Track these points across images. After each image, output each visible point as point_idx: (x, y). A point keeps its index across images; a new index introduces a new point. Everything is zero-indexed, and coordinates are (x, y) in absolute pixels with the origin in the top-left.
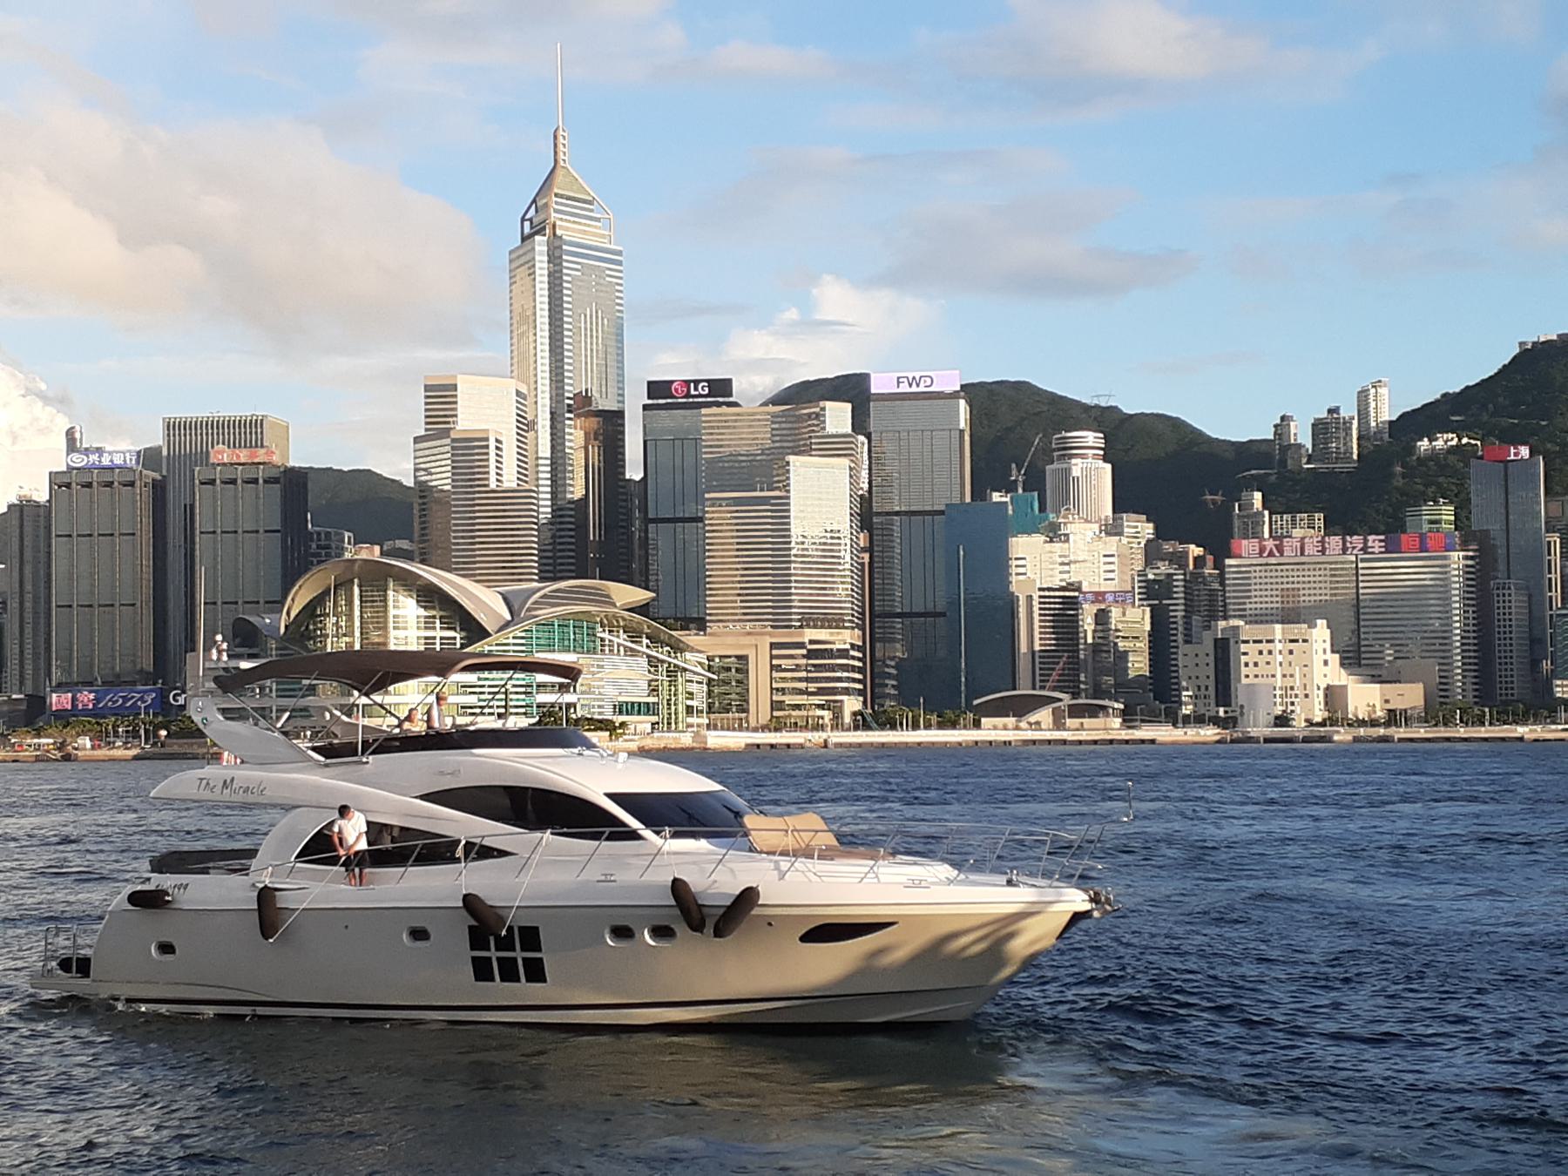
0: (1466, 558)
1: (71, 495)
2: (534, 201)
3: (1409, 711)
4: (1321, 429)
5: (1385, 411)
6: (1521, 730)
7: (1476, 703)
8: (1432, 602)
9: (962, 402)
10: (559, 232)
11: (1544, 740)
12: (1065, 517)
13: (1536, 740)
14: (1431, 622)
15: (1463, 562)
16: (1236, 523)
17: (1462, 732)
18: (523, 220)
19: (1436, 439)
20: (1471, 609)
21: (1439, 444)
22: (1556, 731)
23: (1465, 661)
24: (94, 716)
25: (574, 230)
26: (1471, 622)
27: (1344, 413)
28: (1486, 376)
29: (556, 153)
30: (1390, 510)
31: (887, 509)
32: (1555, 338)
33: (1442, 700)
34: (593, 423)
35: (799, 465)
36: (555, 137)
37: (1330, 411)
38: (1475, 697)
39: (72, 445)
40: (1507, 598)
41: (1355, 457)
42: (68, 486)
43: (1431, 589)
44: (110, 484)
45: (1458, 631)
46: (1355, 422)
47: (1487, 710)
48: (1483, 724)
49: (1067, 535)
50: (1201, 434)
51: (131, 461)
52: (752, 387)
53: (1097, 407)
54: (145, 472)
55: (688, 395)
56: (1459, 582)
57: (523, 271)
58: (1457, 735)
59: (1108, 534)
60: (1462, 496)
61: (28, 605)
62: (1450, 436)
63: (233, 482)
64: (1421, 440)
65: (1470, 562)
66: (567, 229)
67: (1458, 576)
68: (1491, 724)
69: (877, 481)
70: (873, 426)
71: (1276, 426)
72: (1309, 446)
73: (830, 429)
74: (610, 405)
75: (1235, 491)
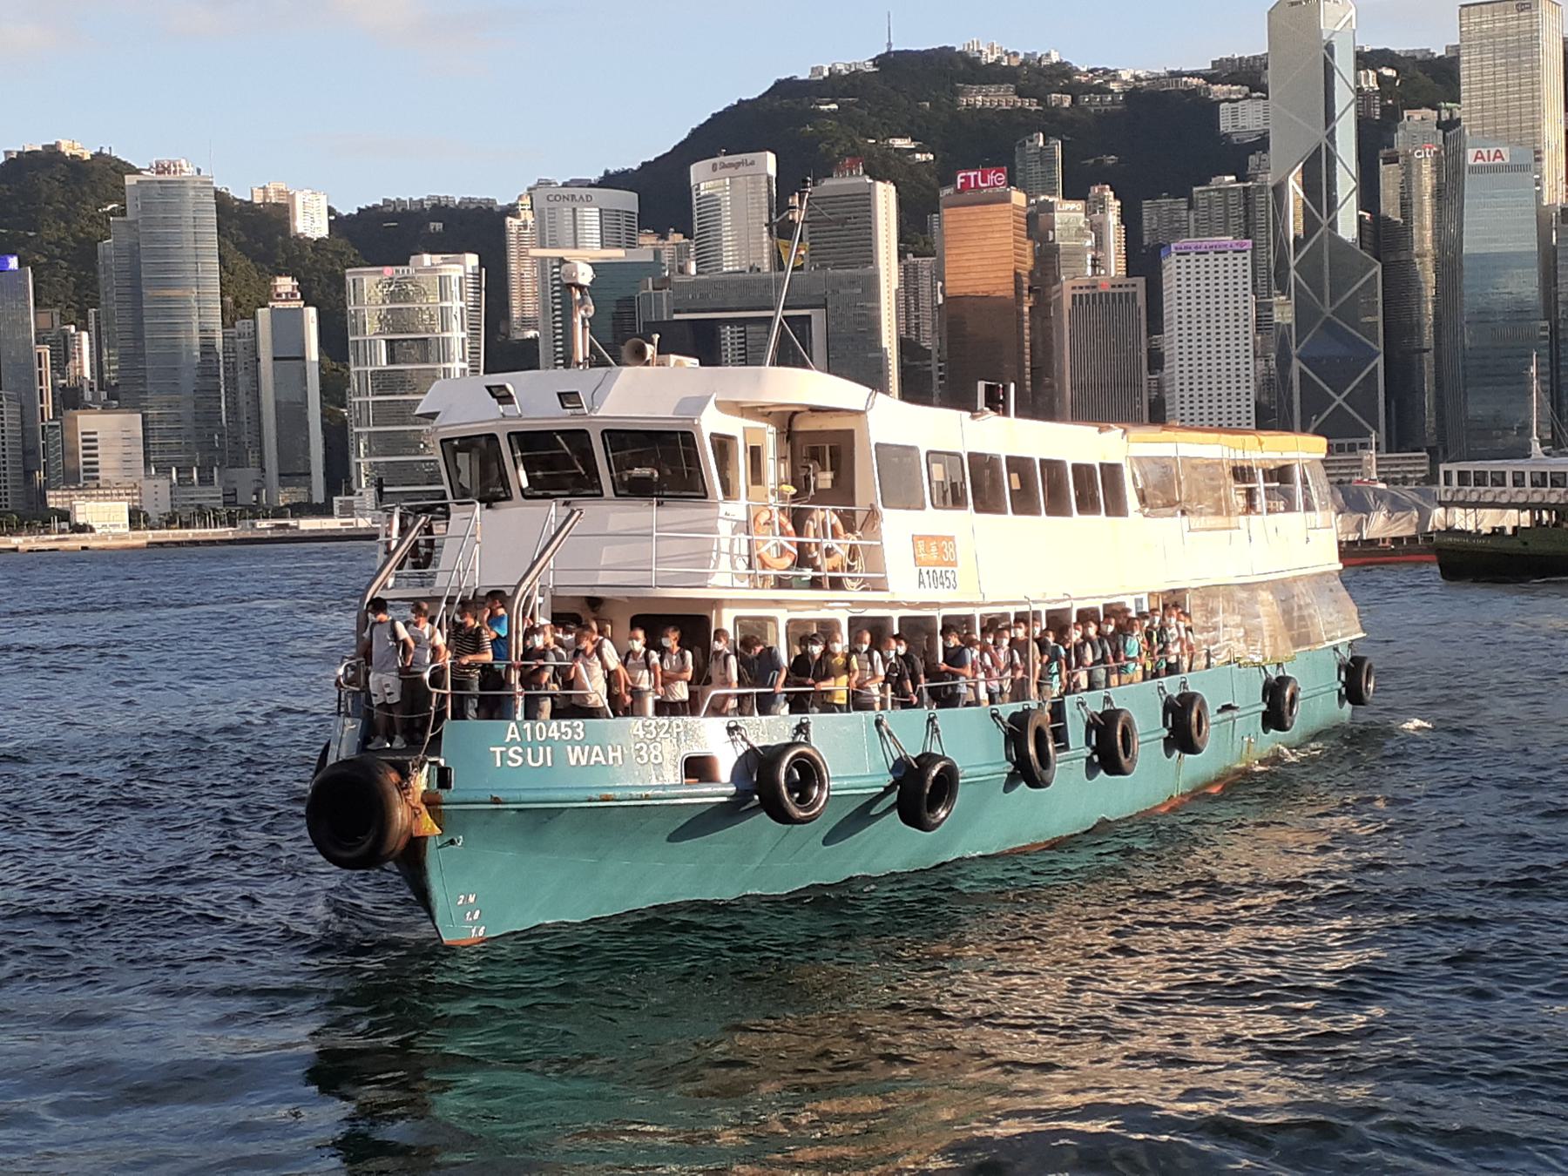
6: (16, 541)
13: (30, 551)
22: (50, 541)
32: (40, 149)
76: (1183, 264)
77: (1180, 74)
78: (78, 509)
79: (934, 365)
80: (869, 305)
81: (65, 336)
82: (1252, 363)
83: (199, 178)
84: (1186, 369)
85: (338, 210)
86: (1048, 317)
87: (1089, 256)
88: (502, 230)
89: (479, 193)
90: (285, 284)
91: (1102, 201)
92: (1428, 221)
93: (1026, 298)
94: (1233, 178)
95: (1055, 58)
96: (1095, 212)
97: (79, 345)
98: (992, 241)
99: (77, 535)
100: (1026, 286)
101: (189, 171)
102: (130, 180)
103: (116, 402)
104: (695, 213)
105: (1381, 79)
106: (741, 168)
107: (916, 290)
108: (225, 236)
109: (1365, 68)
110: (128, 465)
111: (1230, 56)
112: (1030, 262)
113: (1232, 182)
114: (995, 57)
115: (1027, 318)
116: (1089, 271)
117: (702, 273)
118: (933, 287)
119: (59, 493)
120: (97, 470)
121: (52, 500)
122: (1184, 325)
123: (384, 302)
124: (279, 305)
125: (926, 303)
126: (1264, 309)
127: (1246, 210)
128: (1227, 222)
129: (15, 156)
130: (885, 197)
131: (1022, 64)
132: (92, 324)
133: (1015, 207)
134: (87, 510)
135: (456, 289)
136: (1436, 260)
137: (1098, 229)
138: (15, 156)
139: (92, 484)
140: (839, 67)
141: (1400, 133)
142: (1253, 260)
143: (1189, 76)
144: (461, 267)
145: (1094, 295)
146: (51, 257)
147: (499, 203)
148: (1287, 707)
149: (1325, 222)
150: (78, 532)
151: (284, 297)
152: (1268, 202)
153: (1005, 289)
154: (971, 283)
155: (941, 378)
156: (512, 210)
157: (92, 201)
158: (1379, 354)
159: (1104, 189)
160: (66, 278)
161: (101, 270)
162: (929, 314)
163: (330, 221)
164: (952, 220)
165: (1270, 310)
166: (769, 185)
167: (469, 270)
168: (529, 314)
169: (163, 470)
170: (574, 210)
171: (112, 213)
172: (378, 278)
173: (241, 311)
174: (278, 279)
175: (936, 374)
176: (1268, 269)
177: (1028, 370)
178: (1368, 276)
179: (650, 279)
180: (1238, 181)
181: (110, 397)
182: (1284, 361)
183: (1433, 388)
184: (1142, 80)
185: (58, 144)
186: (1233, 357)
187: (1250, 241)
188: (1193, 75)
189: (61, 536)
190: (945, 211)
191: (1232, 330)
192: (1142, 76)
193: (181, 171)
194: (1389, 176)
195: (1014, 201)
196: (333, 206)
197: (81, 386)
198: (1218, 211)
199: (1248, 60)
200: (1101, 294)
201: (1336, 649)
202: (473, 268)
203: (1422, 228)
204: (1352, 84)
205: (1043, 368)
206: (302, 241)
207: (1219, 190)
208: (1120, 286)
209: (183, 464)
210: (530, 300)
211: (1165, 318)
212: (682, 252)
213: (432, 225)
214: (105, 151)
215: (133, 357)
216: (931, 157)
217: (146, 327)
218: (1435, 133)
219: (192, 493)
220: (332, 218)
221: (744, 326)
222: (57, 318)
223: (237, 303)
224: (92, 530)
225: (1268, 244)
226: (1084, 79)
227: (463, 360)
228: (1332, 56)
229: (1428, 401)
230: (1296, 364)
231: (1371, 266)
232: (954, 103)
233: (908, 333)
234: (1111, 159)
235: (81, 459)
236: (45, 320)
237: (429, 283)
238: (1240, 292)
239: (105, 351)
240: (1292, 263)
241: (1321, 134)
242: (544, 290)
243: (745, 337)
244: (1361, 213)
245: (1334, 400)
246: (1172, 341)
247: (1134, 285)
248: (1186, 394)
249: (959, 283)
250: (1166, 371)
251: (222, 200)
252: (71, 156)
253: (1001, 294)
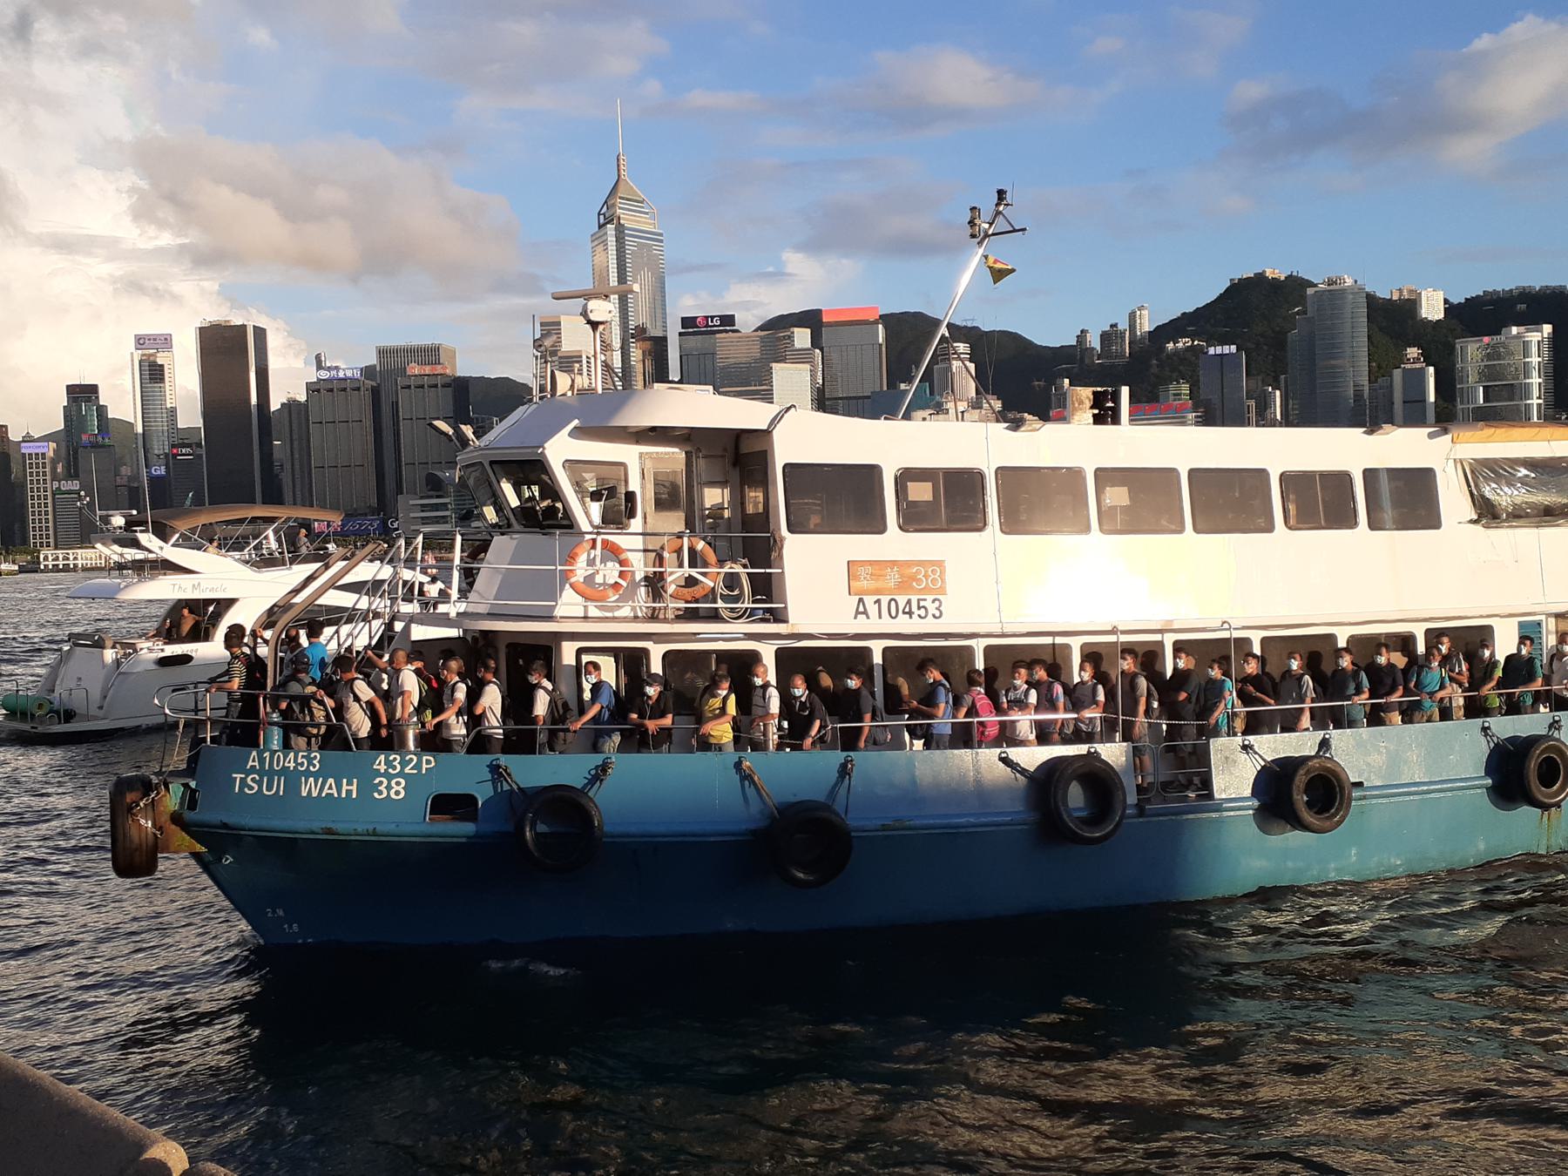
1: (320, 398)
2: (606, 202)
4: (1105, 337)
5: (1146, 325)
9: (880, 326)
10: (622, 221)
12: (946, 398)
16: (1053, 398)
18: (599, 214)
21: (1180, 345)
24: (342, 536)
25: (632, 221)
27: (1120, 327)
29: (619, 170)
30: (1150, 388)
31: (835, 395)
34: (648, 344)
35: (777, 368)
36: (618, 160)
37: (1111, 326)
39: (319, 367)
41: (1127, 355)
42: (318, 391)
44: (344, 390)
46: (1127, 333)
49: (947, 410)
50: (1031, 343)
51: (357, 374)
52: (748, 321)
53: (966, 327)
54: (366, 381)
55: (707, 326)
57: (601, 248)
59: (973, 408)
61: (297, 467)
63: (422, 387)
66: (627, 220)
69: (828, 378)
70: (824, 342)
71: (1078, 337)
72: (1099, 348)
73: (798, 345)
74: (660, 334)
75: (1053, 378)
85: (1451, 300)
90: (1413, 352)
101: (1349, 282)
102: (1310, 291)
124: (1408, 366)
135: (1534, 349)
144: (1540, 334)
163: (1445, 308)
167: (1546, 335)
171: (1298, 313)
172: (1478, 346)
173: (1382, 371)
185: (1264, 272)
206: (1426, 322)
213: (1519, 306)
222: (1260, 383)
223: (1379, 367)
227: (1539, 398)
237: (1516, 347)
239: (1291, 401)
251: (1371, 299)
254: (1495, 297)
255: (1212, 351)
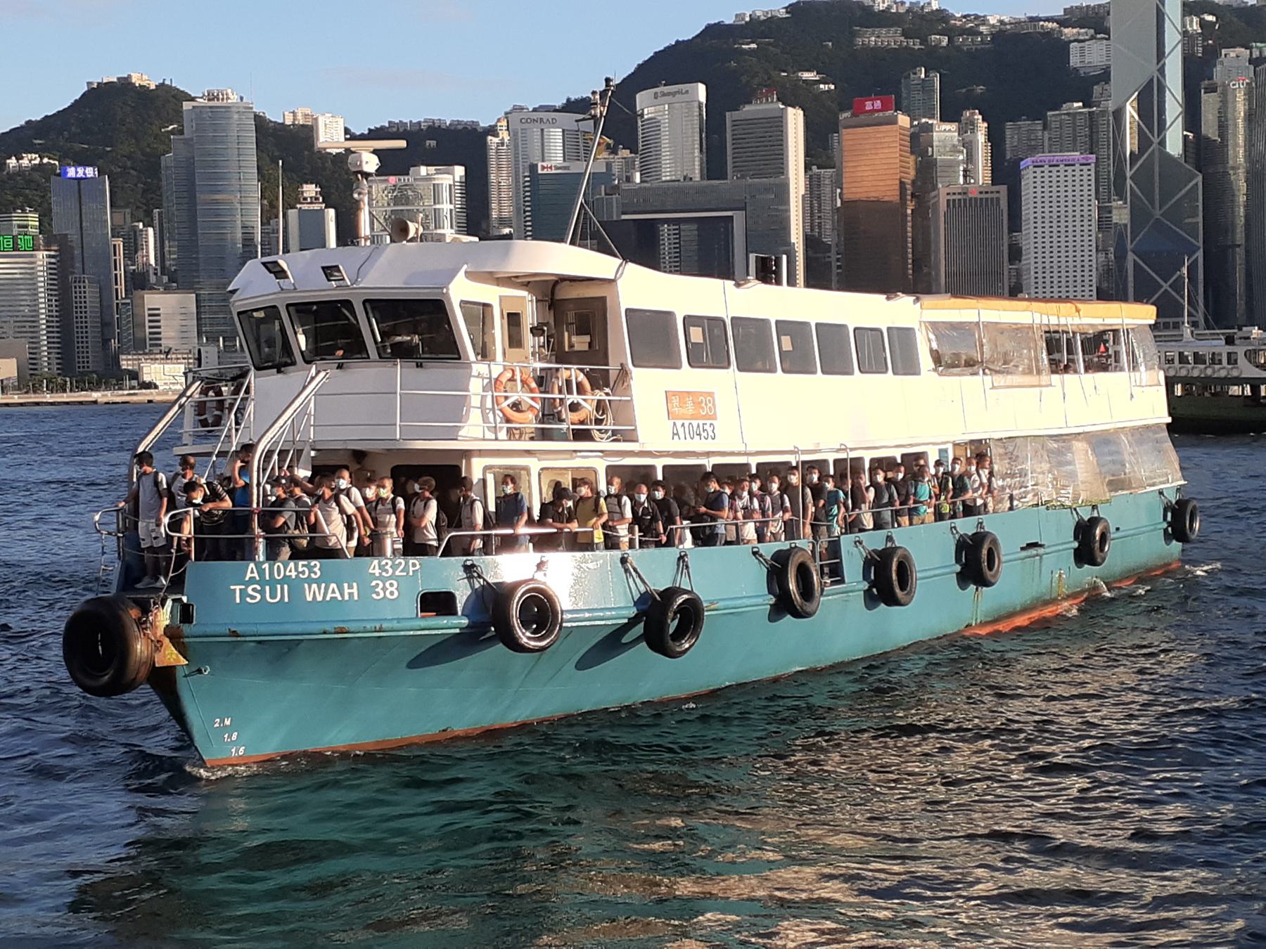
0: (49, 256)
3: (5, 382)
6: (95, 395)
7: (59, 374)
8: (22, 292)
11: (113, 403)
13: (106, 403)
14: (22, 308)
15: (46, 260)
17: (49, 398)
19: (22, 158)
20: (54, 298)
21: (25, 162)
22: (123, 395)
23: (50, 340)
26: (54, 308)
28: (61, 109)
32: (115, 80)
33: (32, 372)
38: (58, 369)
40: (82, 289)
43: (21, 282)
45: (44, 316)
47: (68, 379)
48: (65, 391)
56: (43, 276)
58: (44, 400)
60: (46, 205)
62: (34, 156)
64: (10, 158)
65: (53, 260)
67: (43, 271)
68: (71, 391)
76: (1039, 175)
77: (1038, 19)
78: (145, 370)
79: (833, 256)
80: (780, 208)
81: (135, 230)
82: (1094, 255)
83: (242, 105)
84: (1040, 260)
86: (927, 218)
87: (961, 168)
88: (484, 146)
89: (466, 117)
90: (310, 190)
91: (972, 123)
92: (1241, 141)
93: (909, 202)
94: (1081, 104)
95: (935, 6)
96: (966, 132)
97: (147, 238)
98: (881, 156)
99: (144, 391)
100: (909, 192)
101: (234, 99)
102: (187, 106)
103: (175, 285)
104: (640, 132)
105: (1203, 24)
106: (677, 96)
107: (819, 197)
108: (262, 151)
109: (1190, 14)
110: (185, 335)
111: (1078, 4)
112: (912, 173)
113: (1079, 108)
114: (886, 5)
115: (909, 218)
116: (961, 180)
117: (646, 182)
118: (833, 192)
119: (130, 357)
120: (160, 339)
121: (124, 362)
122: (1039, 225)
123: (389, 205)
124: (305, 207)
125: (827, 207)
126: (1104, 211)
127: (1091, 129)
128: (1075, 140)
129: (95, 86)
130: (795, 120)
131: (908, 11)
132: (156, 222)
133: (902, 128)
134: (152, 371)
135: (445, 195)
136: (1248, 172)
137: (969, 147)
138: (95, 86)
139: (156, 350)
140: (758, 14)
141: (1219, 67)
142: (1097, 172)
143: (1044, 21)
144: (451, 177)
145: (965, 200)
146: (125, 168)
147: (482, 125)
148: (1097, 545)
149: (1156, 140)
150: (145, 388)
151: (309, 200)
152: (1108, 124)
153: (892, 195)
154: (866, 189)
155: (839, 267)
156: (492, 131)
157: (156, 122)
158: (1199, 248)
159: (973, 114)
160: (136, 185)
161: (164, 178)
162: (829, 216)
164: (850, 139)
165: (1110, 212)
166: (700, 107)
167: (457, 179)
168: (505, 214)
169: (213, 339)
170: (542, 130)
171: (172, 132)
172: (384, 186)
174: (305, 186)
175: (835, 264)
176: (1109, 179)
177: (910, 261)
178: (1191, 184)
179: (603, 187)
180: (1084, 106)
181: (171, 280)
182: (1121, 257)
183: (1243, 276)
184: (1006, 24)
185: (130, 76)
186: (1071, 252)
187: (1094, 156)
188: (1048, 19)
189: (132, 392)
190: (844, 131)
191: (1078, 229)
192: (1007, 20)
193: (228, 98)
194: (1209, 103)
195: (900, 123)
196: (349, 127)
197: (148, 271)
198: (1067, 131)
199: (1094, 7)
200: (971, 199)
201: (1161, 493)
202: (461, 177)
203: (1236, 145)
204: (1179, 29)
205: (923, 259)
206: (323, 156)
207: (1068, 114)
208: (987, 193)
209: (228, 335)
210: (506, 203)
211: (1023, 218)
212: (629, 164)
213: (428, 142)
214: (167, 82)
215: (189, 246)
216: (832, 87)
217: (199, 224)
218: (1247, 67)
219: (237, 357)
220: (348, 136)
221: (679, 224)
222: (128, 216)
224: (156, 387)
225: (1109, 159)
226: (959, 23)
228: (1163, 5)
229: (1240, 288)
230: (1131, 257)
231: (1193, 177)
232: (851, 43)
233: (812, 230)
234: (980, 89)
235: (148, 330)
236: (119, 218)
237: (422, 188)
238: (1085, 198)
239: (167, 242)
240: (1129, 174)
241: (1153, 68)
242: (517, 193)
243: (679, 234)
244: (1185, 133)
245: (1162, 287)
246: (1029, 238)
247: (998, 192)
248: (1040, 280)
249: (854, 190)
250: (1023, 262)
251: (260, 121)
252: (140, 86)
253: (886, 199)
254: (401, 130)
255: (71, 172)
